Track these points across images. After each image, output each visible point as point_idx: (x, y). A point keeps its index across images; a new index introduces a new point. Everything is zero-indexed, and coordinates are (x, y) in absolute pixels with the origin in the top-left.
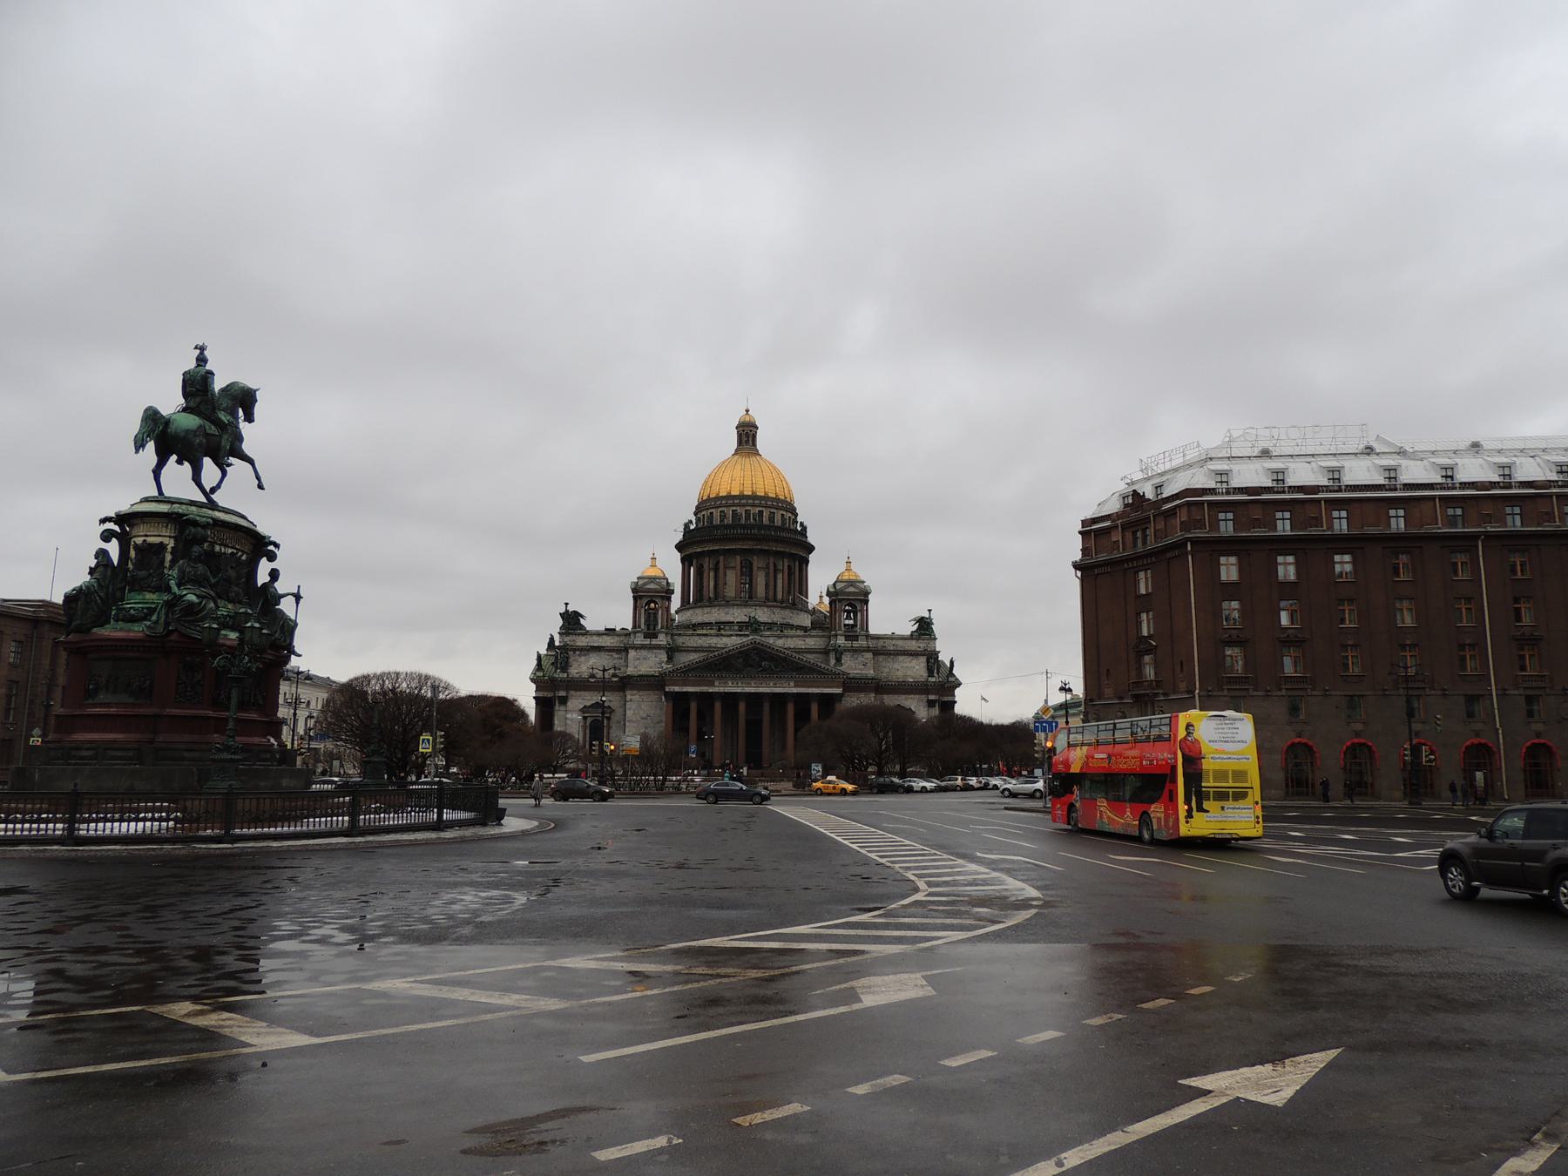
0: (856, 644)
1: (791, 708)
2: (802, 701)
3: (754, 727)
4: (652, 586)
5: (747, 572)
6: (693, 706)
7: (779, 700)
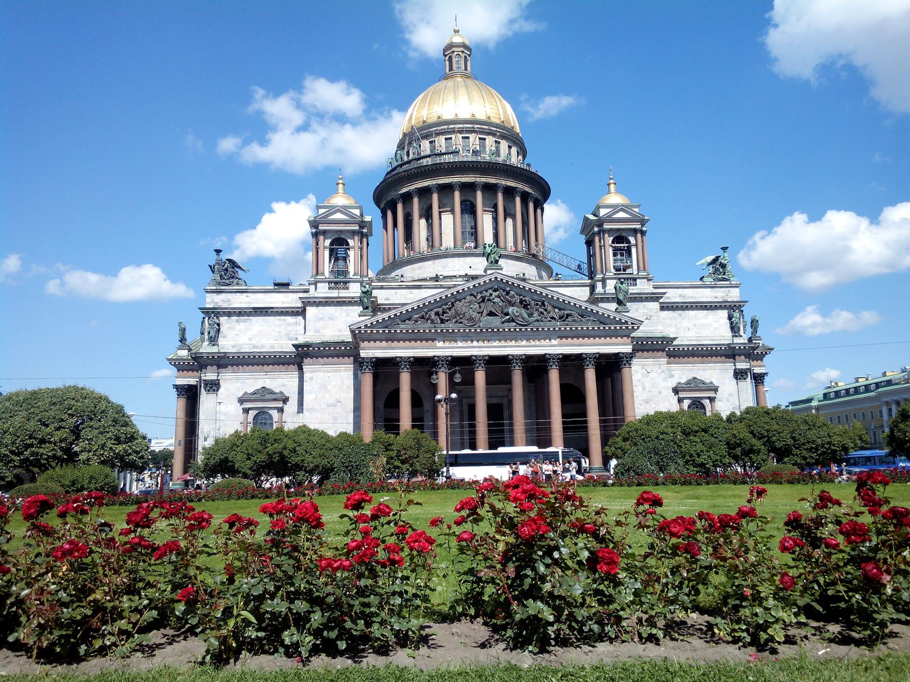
0: (633, 290)
1: (554, 376)
2: (572, 365)
3: (499, 413)
4: (338, 216)
5: (469, 209)
6: (405, 379)
7: (536, 368)
